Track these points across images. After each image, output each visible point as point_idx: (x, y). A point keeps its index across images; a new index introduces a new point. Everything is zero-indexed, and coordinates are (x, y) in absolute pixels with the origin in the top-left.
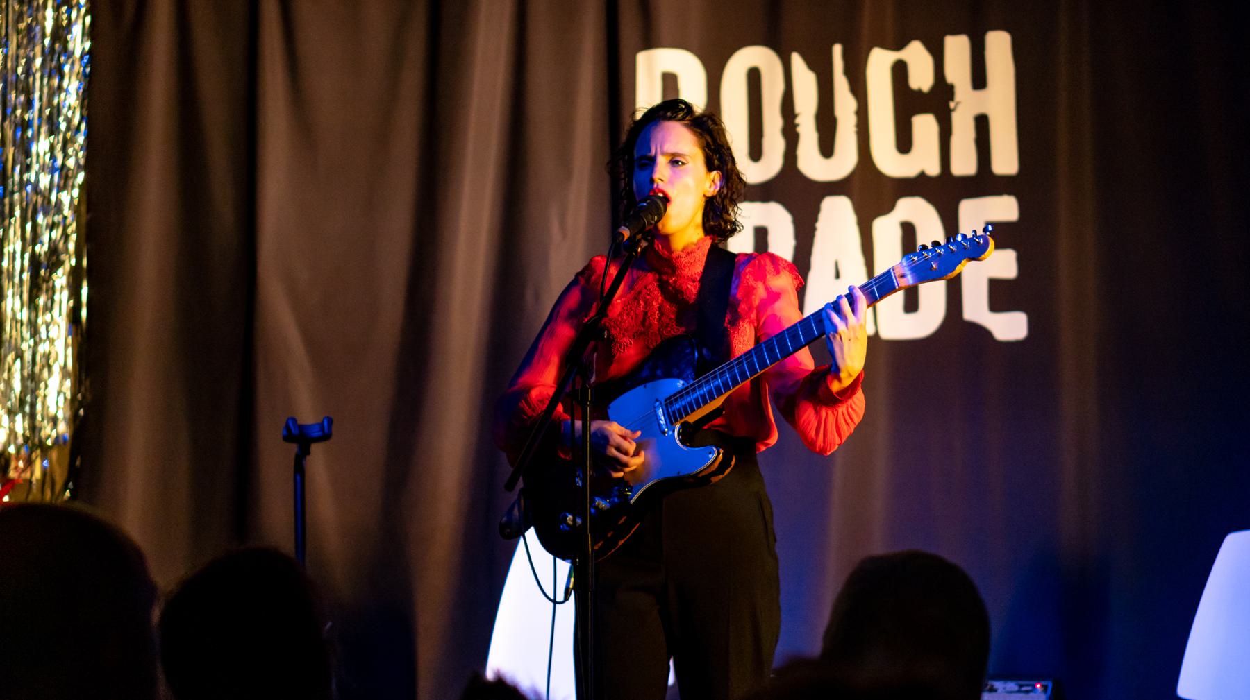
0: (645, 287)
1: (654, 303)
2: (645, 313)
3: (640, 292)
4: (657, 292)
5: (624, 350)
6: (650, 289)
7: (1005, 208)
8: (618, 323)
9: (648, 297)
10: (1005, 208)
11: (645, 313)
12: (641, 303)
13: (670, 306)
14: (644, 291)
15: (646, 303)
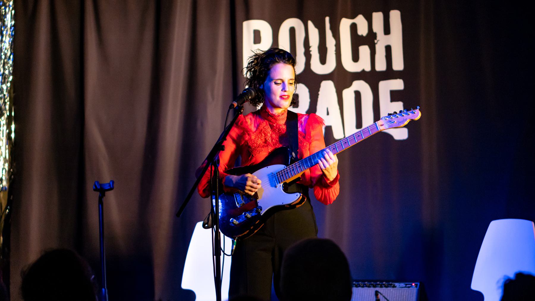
0: (264, 127)
1: (268, 134)
2: (265, 139)
3: (262, 130)
4: (269, 130)
5: (259, 153)
6: (265, 129)
7: (398, 84)
8: (255, 142)
9: (265, 132)
10: (398, 84)
11: (265, 139)
12: (263, 135)
13: (275, 135)
14: (263, 130)
15: (265, 134)
